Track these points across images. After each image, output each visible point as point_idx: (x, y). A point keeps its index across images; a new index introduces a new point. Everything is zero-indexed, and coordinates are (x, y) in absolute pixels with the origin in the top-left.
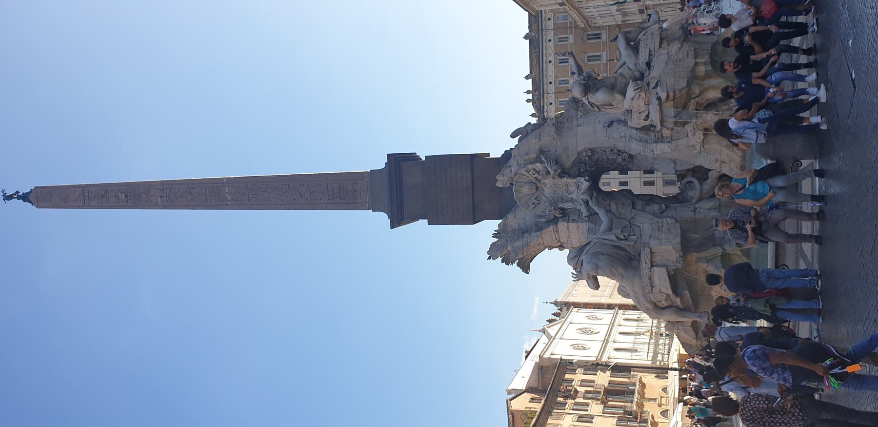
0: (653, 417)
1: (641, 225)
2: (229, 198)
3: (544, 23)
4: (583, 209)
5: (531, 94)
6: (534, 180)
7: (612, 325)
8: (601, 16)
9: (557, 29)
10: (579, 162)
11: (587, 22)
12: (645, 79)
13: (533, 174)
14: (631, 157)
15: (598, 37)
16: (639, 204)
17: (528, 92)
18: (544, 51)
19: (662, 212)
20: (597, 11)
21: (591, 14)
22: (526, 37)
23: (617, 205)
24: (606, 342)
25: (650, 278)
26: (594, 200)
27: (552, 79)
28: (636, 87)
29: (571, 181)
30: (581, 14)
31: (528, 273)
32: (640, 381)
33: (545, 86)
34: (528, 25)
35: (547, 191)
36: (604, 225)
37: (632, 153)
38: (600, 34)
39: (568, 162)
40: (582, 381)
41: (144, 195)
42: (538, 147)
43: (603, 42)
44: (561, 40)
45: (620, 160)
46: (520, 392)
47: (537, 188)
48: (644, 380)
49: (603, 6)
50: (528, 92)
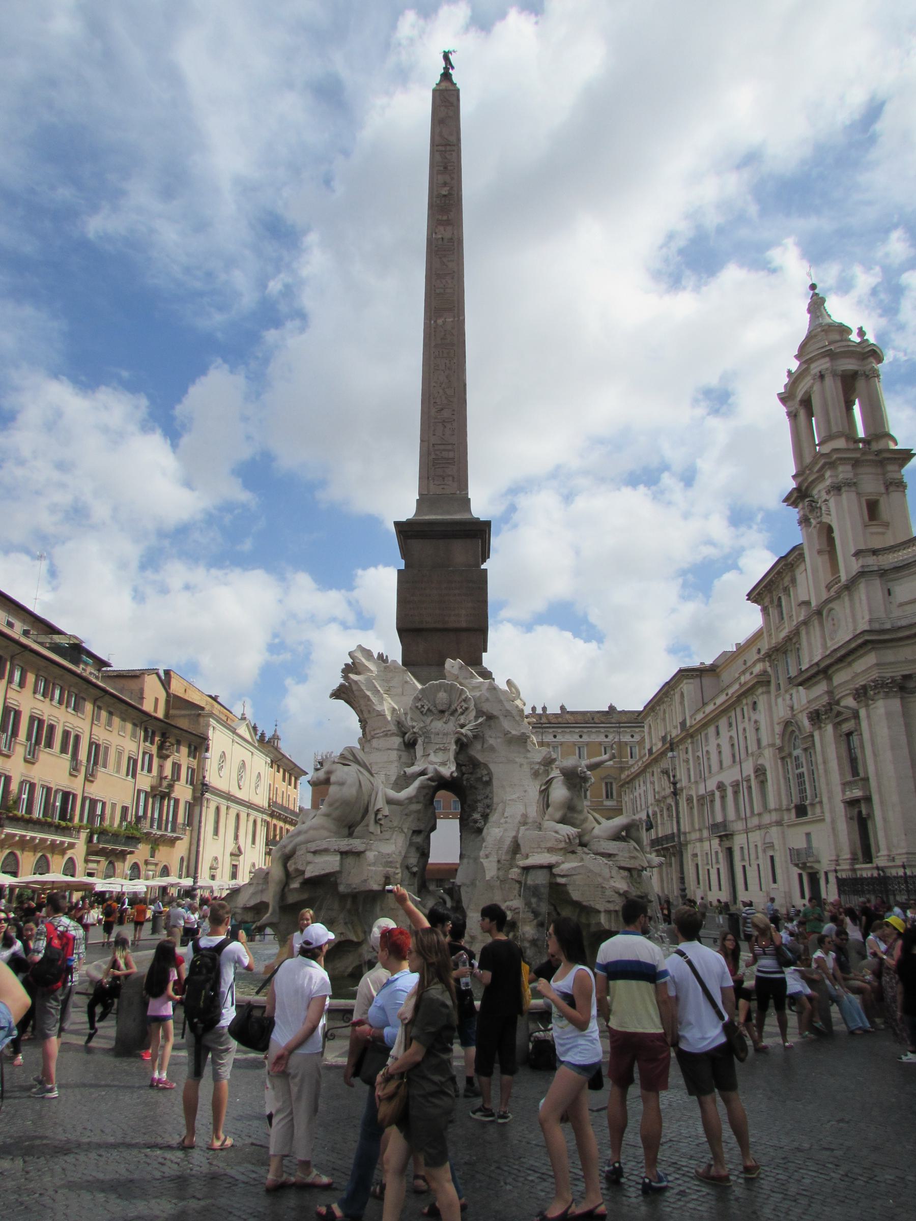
0: (132, 853)
1: (392, 841)
2: (440, 322)
3: (628, 730)
4: (416, 769)
5: (541, 712)
6: (453, 707)
7: (250, 806)
8: (634, 801)
10: (475, 764)
11: (628, 783)
12: (580, 848)
13: (461, 707)
14: (480, 831)
15: (609, 796)
16: (419, 839)
17: (544, 709)
18: (594, 730)
19: (408, 868)
20: (640, 795)
21: (637, 787)
22: (612, 708)
23: (418, 812)
24: (229, 797)
25: (326, 851)
26: (426, 782)
28: (571, 837)
29: (451, 755)
30: (638, 775)
31: (331, 697)
33: (551, 730)
35: (438, 725)
36: (392, 794)
37: (485, 831)
38: (612, 797)
39: (476, 752)
40: (179, 766)
41: (445, 218)
42: (495, 713)
43: (602, 802)
45: (476, 816)
46: (167, 687)
47: (442, 712)
48: (178, 842)
49: (646, 802)
50: (544, 709)
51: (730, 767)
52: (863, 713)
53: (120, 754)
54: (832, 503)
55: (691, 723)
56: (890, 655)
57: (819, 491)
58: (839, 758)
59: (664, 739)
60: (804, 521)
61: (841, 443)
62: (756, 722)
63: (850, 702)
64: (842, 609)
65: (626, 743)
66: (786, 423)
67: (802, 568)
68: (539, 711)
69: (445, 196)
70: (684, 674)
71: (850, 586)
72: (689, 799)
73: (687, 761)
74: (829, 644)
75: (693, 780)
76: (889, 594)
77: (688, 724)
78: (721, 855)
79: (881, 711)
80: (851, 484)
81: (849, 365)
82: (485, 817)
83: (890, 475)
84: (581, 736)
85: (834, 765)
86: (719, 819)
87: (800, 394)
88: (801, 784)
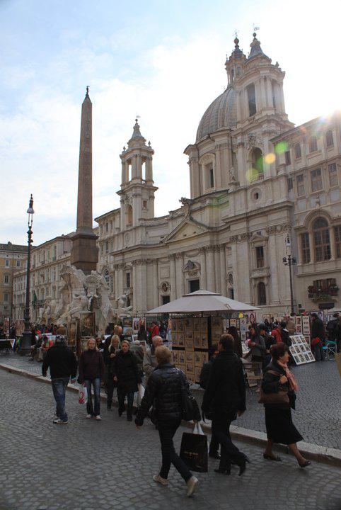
4: (89, 295)
22: (9, 242)
35: (90, 285)
44: (7, 261)
52: (134, 268)
56: (144, 252)
57: (130, 194)
58: (123, 281)
59: (43, 263)
60: (122, 201)
61: (139, 181)
63: (130, 264)
64: (132, 235)
66: (121, 165)
67: (118, 216)
70: (58, 239)
71: (136, 228)
72: (54, 288)
73: (55, 273)
74: (125, 244)
75: (57, 280)
77: (57, 259)
79: (140, 269)
81: (145, 154)
85: (121, 283)
87: (128, 157)
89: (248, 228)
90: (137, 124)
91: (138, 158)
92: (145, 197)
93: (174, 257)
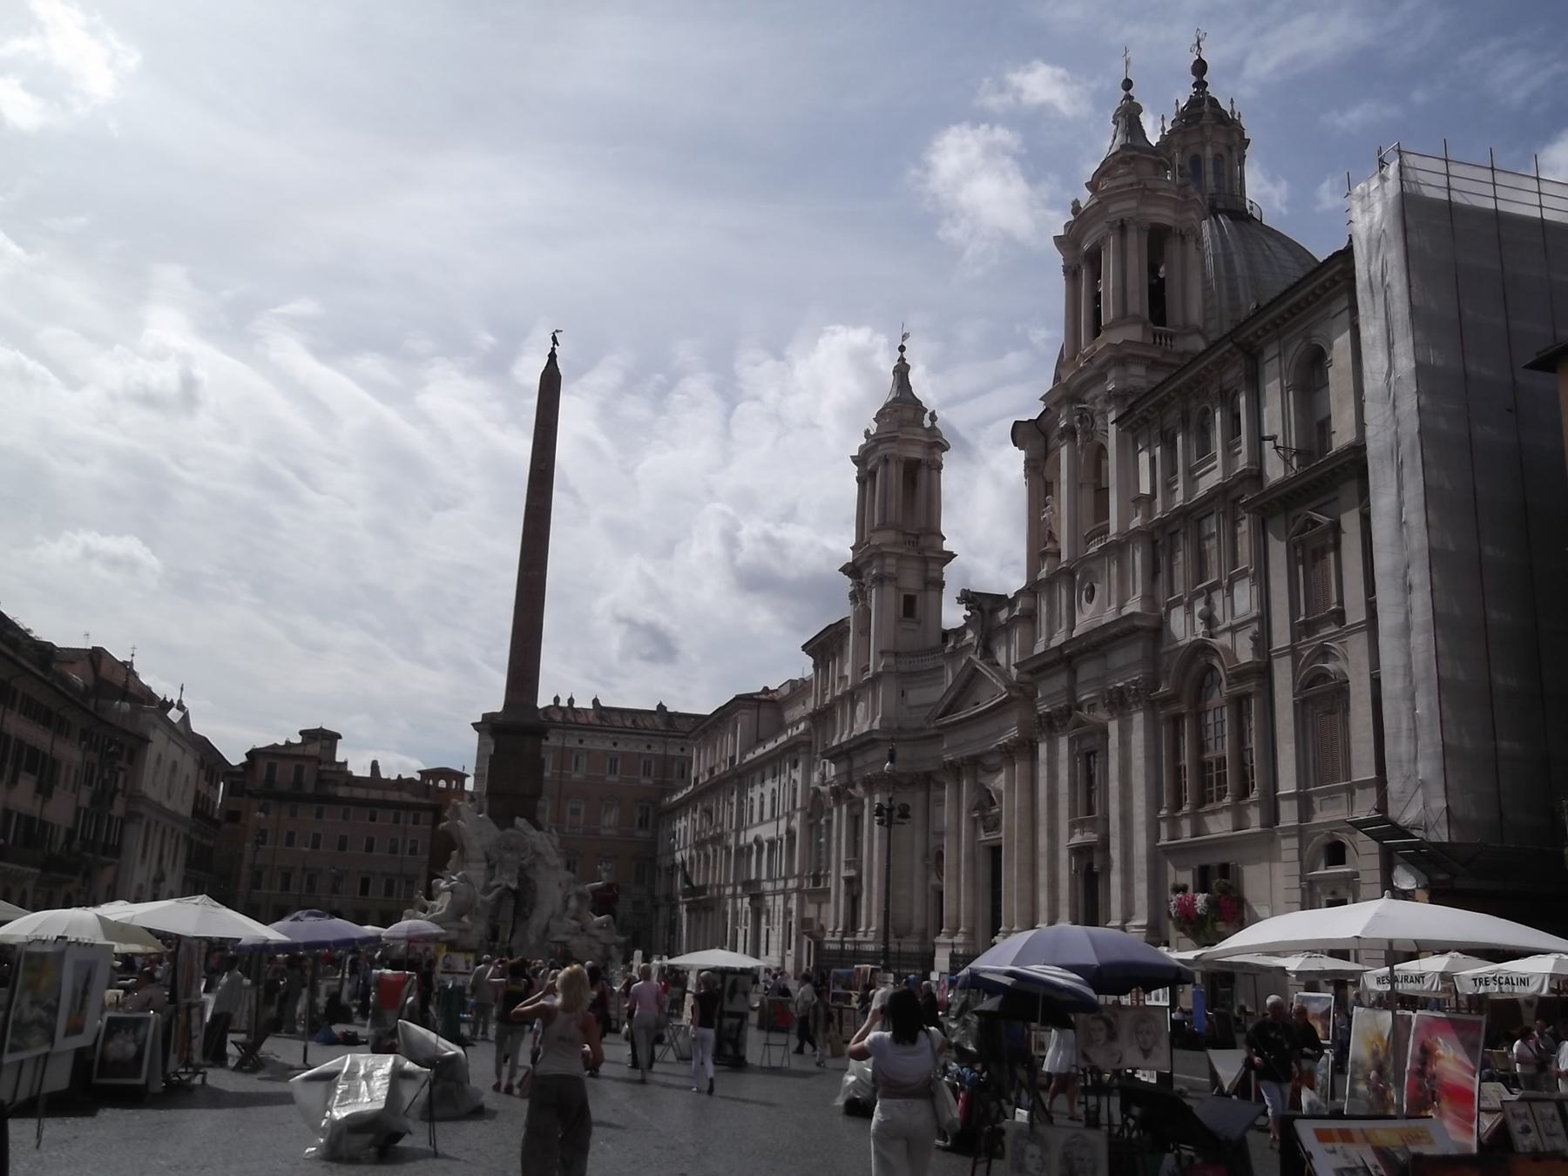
4: (493, 883)
5: (566, 705)
9: (666, 761)
17: (571, 701)
18: (634, 737)
20: (680, 830)
22: (661, 707)
24: (159, 809)
27: (587, 744)
32: (111, 864)
33: (576, 733)
34: (680, 711)
35: (508, 855)
44: (647, 766)
47: (511, 849)
50: (571, 701)
51: (768, 821)
53: (69, 767)
54: (874, 591)
55: (740, 761)
60: (853, 596)
62: (795, 781)
65: (673, 758)
66: (854, 487)
68: (563, 703)
69: (542, 470)
70: (741, 701)
75: (734, 827)
76: (903, 695)
78: (750, 915)
80: (894, 579)
81: (916, 453)
82: (531, 910)
83: (932, 574)
84: (615, 744)
86: (753, 877)
88: (819, 854)
89: (1071, 691)
90: (902, 359)
91: (892, 468)
92: (911, 581)
93: (955, 770)
